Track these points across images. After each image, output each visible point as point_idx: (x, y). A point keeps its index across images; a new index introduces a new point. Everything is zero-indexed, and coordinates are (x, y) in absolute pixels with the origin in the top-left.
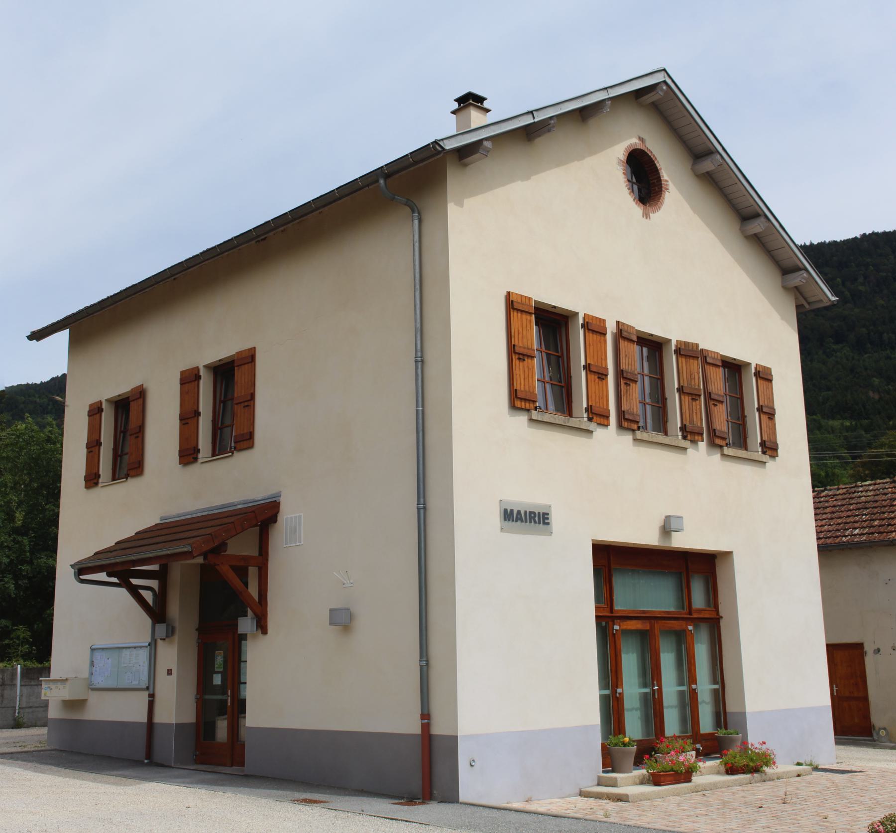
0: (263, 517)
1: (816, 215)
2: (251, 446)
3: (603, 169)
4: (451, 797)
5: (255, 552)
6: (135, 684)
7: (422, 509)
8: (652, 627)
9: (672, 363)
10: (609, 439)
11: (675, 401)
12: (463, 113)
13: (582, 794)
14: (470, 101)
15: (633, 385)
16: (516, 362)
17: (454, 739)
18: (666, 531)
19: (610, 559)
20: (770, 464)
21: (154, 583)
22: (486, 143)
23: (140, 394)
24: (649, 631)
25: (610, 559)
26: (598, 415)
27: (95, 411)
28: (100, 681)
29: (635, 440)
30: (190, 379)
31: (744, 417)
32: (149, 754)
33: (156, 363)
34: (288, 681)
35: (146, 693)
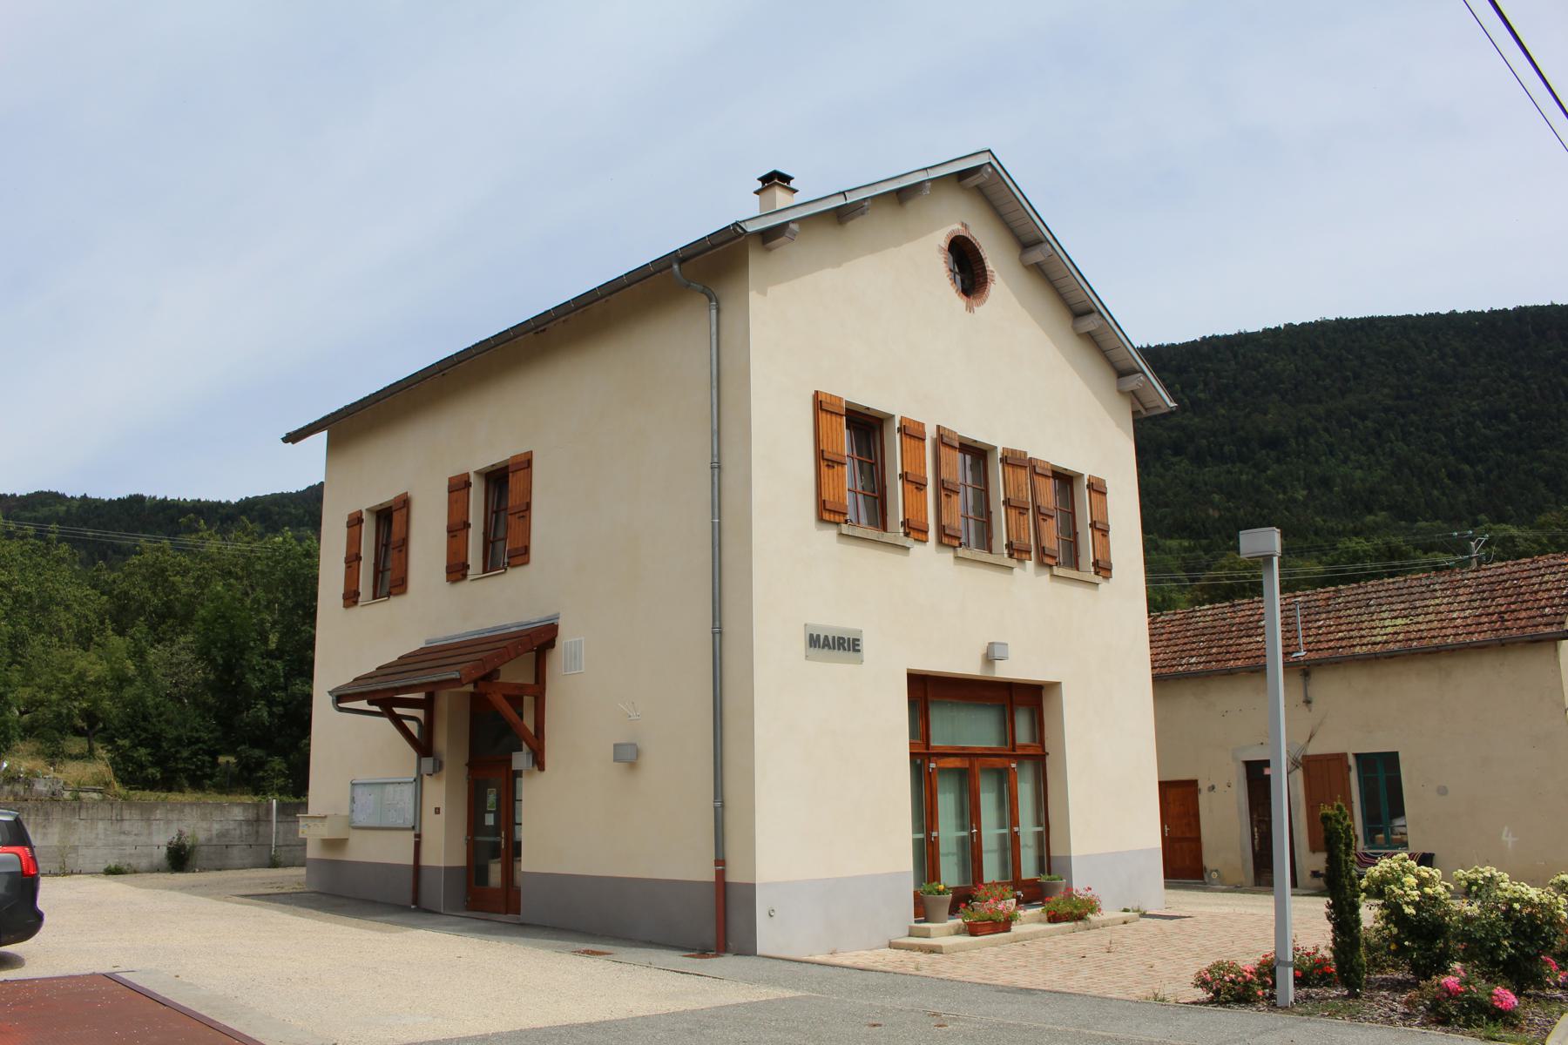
0: (539, 642)
2: (527, 562)
3: (925, 254)
4: (747, 948)
5: (530, 680)
6: (400, 823)
7: (718, 633)
8: (972, 765)
9: (997, 472)
10: (928, 556)
11: (1000, 514)
12: (768, 193)
13: (892, 946)
14: (775, 179)
15: (954, 496)
16: (824, 469)
17: (751, 888)
18: (989, 659)
19: (927, 691)
20: (1104, 585)
21: (419, 713)
22: (792, 226)
23: (404, 503)
24: (968, 769)
25: (927, 691)
26: (915, 530)
27: (355, 522)
28: (361, 819)
29: (956, 558)
30: (459, 486)
31: (1076, 534)
32: (416, 900)
33: (420, 469)
34: (566, 821)
35: (411, 834)
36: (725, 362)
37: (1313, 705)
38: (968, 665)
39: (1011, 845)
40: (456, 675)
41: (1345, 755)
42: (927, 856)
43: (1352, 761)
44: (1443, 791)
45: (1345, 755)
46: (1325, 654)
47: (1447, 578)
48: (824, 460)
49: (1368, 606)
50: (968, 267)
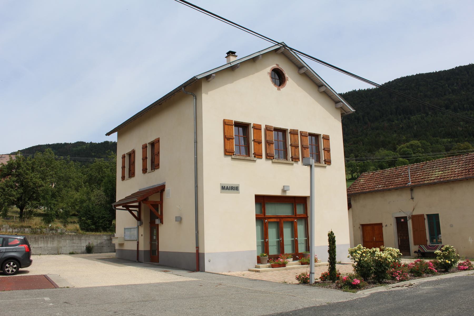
0: (161, 189)
1: (342, 85)
2: (159, 168)
3: (263, 75)
4: (203, 271)
5: (159, 200)
6: (132, 238)
7: (196, 187)
8: (280, 221)
9: (289, 136)
10: (263, 163)
11: (289, 148)
12: (228, 58)
13: (249, 270)
14: (231, 53)
15: (271, 145)
16: (226, 141)
17: (204, 254)
18: (284, 191)
19: (262, 200)
20: (328, 167)
21: (137, 209)
22: (213, 75)
23: (134, 152)
24: (279, 222)
25: (262, 200)
26: (259, 156)
27: (124, 157)
28: (127, 238)
29: (272, 162)
30: (145, 147)
31: (319, 152)
32: (138, 259)
33: (135, 143)
34: (171, 239)
35: (136, 242)
36: (198, 113)
37: (414, 200)
38: (278, 193)
39: (295, 244)
40: (136, 199)
41: (423, 215)
42: (265, 246)
43: (425, 217)
44: (451, 226)
45: (423, 215)
46: (416, 184)
47: (458, 158)
48: (227, 138)
49: (433, 168)
50: (279, 78)
